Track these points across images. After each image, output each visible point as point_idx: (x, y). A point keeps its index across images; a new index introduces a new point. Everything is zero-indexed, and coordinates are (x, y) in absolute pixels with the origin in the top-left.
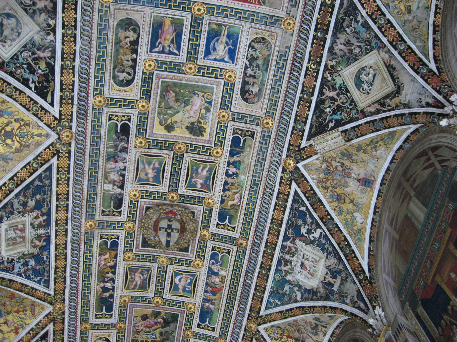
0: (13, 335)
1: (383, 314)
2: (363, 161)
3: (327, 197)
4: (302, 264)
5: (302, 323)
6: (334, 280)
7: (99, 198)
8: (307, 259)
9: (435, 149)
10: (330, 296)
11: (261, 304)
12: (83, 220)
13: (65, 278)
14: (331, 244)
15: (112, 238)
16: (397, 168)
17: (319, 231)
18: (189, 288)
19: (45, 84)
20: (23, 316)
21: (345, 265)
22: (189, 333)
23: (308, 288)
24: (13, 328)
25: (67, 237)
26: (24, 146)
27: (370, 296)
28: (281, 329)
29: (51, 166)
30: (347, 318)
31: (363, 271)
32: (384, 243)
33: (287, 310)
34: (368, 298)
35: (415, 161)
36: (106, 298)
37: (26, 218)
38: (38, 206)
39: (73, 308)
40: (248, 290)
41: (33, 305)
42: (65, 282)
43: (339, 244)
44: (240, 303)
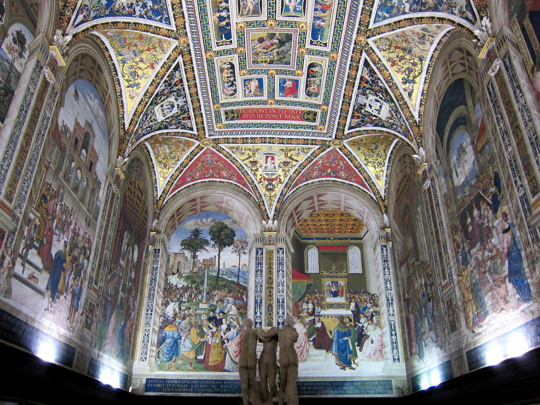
0: (150, 70)
1: (489, 25)
5: (409, 34)
10: (439, 6)
11: (370, 18)
13: (183, 13)
18: (299, 8)
20: (154, 53)
22: (303, 50)
24: (149, 64)
27: (479, 6)
28: (389, 40)
30: (454, 28)
33: (394, 23)
34: (477, 8)
36: (223, 27)
40: (357, 5)
41: (160, 42)
44: (349, 18)
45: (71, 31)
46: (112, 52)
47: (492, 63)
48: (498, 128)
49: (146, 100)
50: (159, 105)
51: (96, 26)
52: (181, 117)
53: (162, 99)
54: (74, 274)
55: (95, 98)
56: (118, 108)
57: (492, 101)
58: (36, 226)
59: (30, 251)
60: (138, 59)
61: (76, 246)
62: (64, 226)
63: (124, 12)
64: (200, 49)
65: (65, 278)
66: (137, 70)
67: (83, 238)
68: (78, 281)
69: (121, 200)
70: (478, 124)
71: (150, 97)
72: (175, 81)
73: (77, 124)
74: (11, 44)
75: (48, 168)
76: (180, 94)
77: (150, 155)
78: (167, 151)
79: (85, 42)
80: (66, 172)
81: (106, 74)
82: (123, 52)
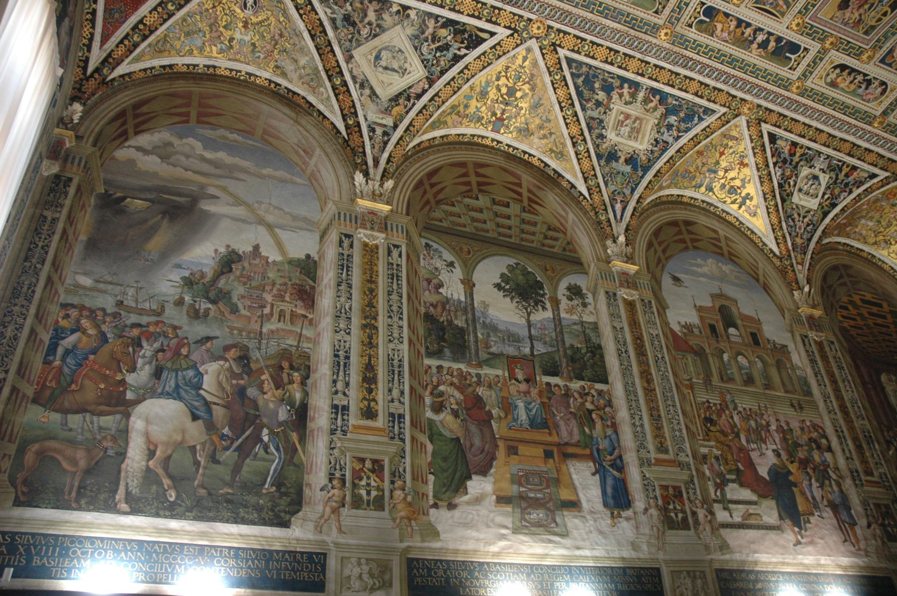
0: (746, 171)
7: (635, 12)
12: (654, 41)
13: (715, 88)
15: (699, 13)
19: (466, 36)
20: (731, 151)
25: (664, 68)
26: (531, 80)
29: (566, 58)
36: (777, 48)
37: (616, 107)
38: (608, 89)
39: (761, 92)
42: (720, 90)
45: (619, 229)
46: (689, 193)
49: (772, 203)
50: (795, 193)
51: (640, 197)
52: (841, 176)
53: (792, 183)
54: (817, 481)
55: (705, 259)
56: (750, 239)
58: (717, 458)
59: (727, 489)
60: (721, 173)
61: (797, 445)
62: (760, 434)
63: (656, 154)
64: (777, 95)
65: (803, 493)
66: (732, 184)
67: (802, 429)
68: (831, 486)
69: (839, 342)
71: (774, 196)
72: (786, 151)
73: (700, 309)
74: (568, 305)
75: (691, 387)
76: (809, 158)
77: (852, 247)
78: (871, 224)
79: (648, 217)
80: (720, 373)
81: (702, 220)
82: (699, 181)
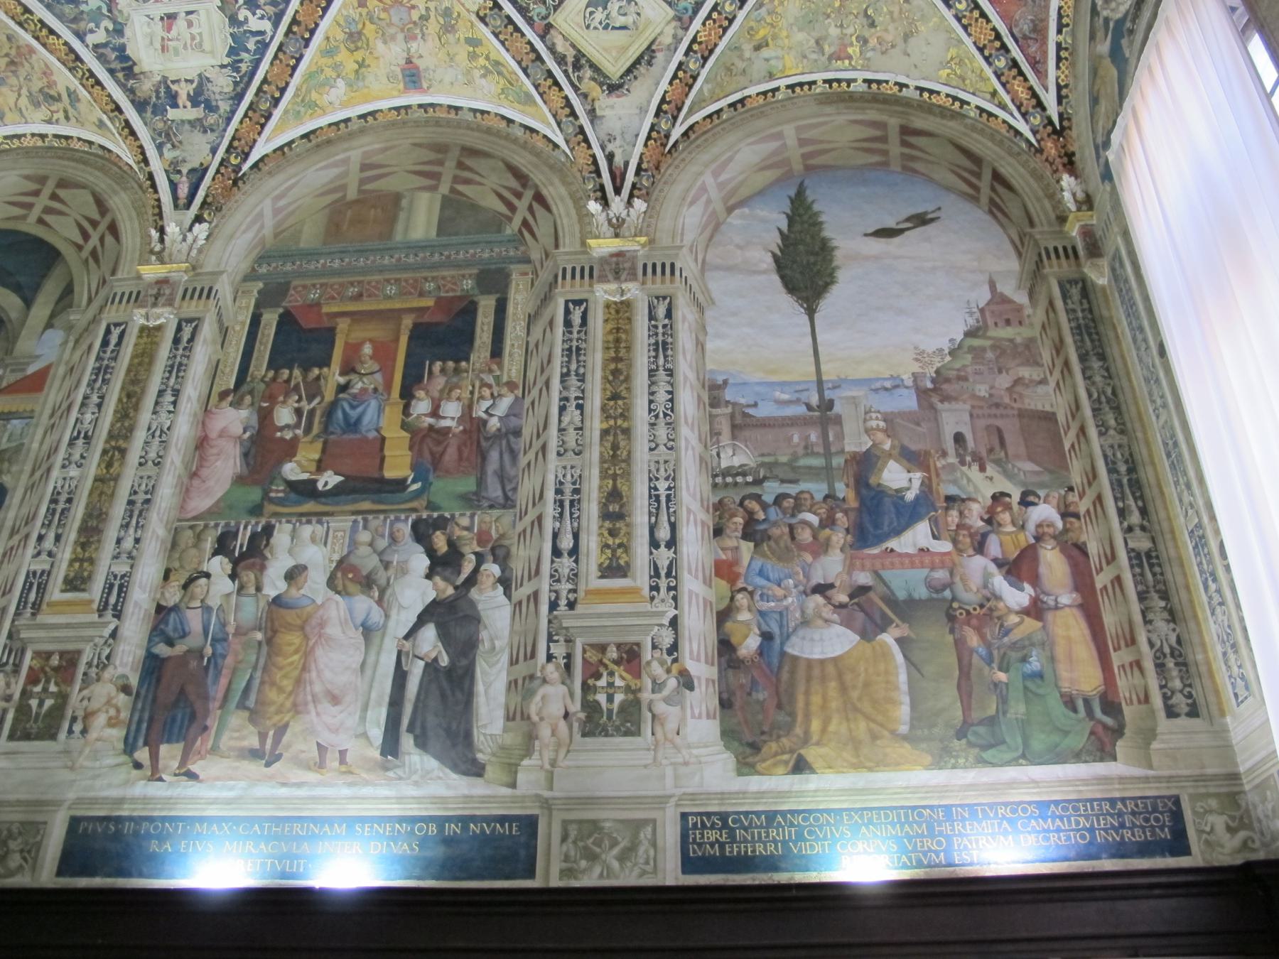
1: (201, 242)
2: (451, 58)
3: (345, 13)
4: (171, 17)
6: (189, 104)
8: (190, 24)
9: (539, 198)
10: (149, 109)
14: (256, 64)
16: (469, 127)
17: (266, 26)
21: (233, 112)
23: (128, 52)
31: (246, 156)
32: (322, 169)
35: (501, 164)
43: (265, 81)
47: (155, 305)
48: (74, 414)
57: (99, 358)
70: (28, 364)
